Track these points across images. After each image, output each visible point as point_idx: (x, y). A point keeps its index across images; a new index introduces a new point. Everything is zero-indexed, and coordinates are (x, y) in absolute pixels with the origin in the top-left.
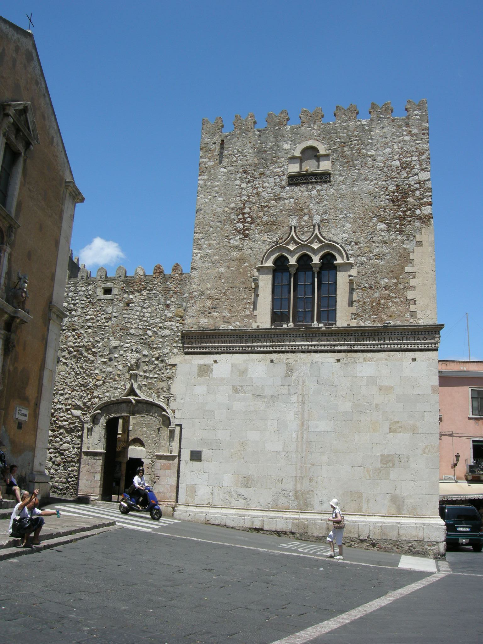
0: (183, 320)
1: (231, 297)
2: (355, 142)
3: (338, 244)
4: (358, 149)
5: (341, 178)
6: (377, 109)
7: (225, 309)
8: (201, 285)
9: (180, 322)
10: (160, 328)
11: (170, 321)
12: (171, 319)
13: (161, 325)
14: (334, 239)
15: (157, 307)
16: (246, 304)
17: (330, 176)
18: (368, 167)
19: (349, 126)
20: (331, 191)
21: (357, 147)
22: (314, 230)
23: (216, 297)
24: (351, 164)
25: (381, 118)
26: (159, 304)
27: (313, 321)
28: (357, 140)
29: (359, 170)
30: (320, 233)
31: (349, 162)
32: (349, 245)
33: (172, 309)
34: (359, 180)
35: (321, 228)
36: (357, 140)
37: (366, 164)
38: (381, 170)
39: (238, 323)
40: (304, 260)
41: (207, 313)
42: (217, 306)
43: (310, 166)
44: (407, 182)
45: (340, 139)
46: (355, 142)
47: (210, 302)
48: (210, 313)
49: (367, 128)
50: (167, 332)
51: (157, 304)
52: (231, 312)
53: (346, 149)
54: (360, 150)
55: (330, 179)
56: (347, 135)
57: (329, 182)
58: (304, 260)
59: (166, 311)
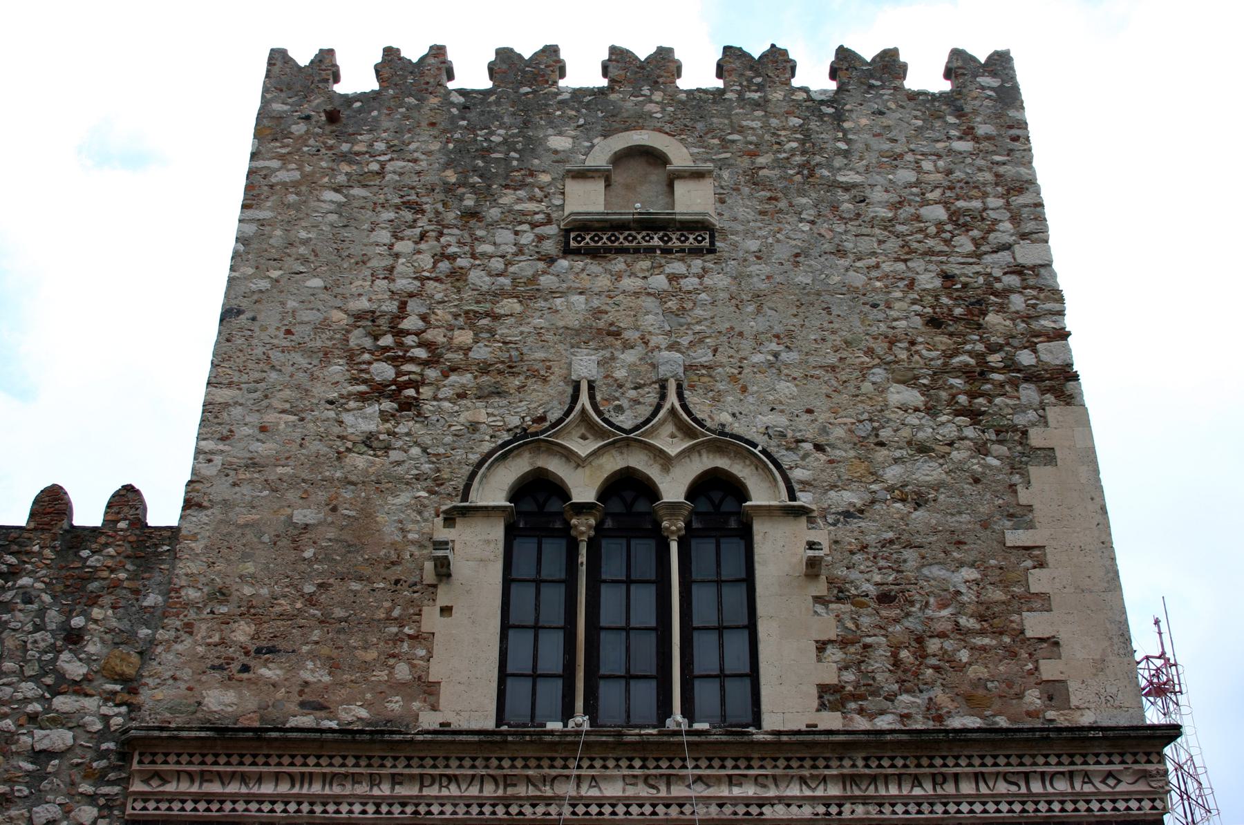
0: (134, 692)
1: (339, 613)
2: (794, 145)
3: (755, 446)
4: (802, 166)
5: (753, 245)
6: (857, 64)
7: (313, 656)
8: (220, 566)
9: (118, 699)
10: (33, 718)
11: (76, 693)
12: (78, 688)
13: (36, 707)
14: (737, 428)
15: (30, 638)
16: (397, 639)
17: (712, 237)
18: (841, 218)
19: (767, 101)
20: (718, 280)
21: (798, 159)
22: (663, 396)
23: (278, 609)
24: (783, 204)
25: (871, 87)
26: (37, 628)
27: (669, 713)
28: (796, 140)
29: (813, 223)
30: (685, 407)
31: (776, 199)
32: (788, 449)
33: (93, 647)
34: (815, 252)
35: (687, 393)
36: (796, 140)
37: (835, 208)
38: (885, 228)
39: (364, 713)
40: (628, 490)
41: (235, 667)
42: (281, 644)
43: (642, 200)
44: (978, 268)
45: (740, 132)
46: (794, 145)
47: (251, 629)
48: (245, 669)
49: (831, 110)
50: (60, 738)
51: (29, 627)
52: (333, 666)
53: (761, 160)
54: (809, 171)
55: (712, 243)
56: (766, 126)
57: (712, 250)
58: (628, 490)
59: (65, 656)
